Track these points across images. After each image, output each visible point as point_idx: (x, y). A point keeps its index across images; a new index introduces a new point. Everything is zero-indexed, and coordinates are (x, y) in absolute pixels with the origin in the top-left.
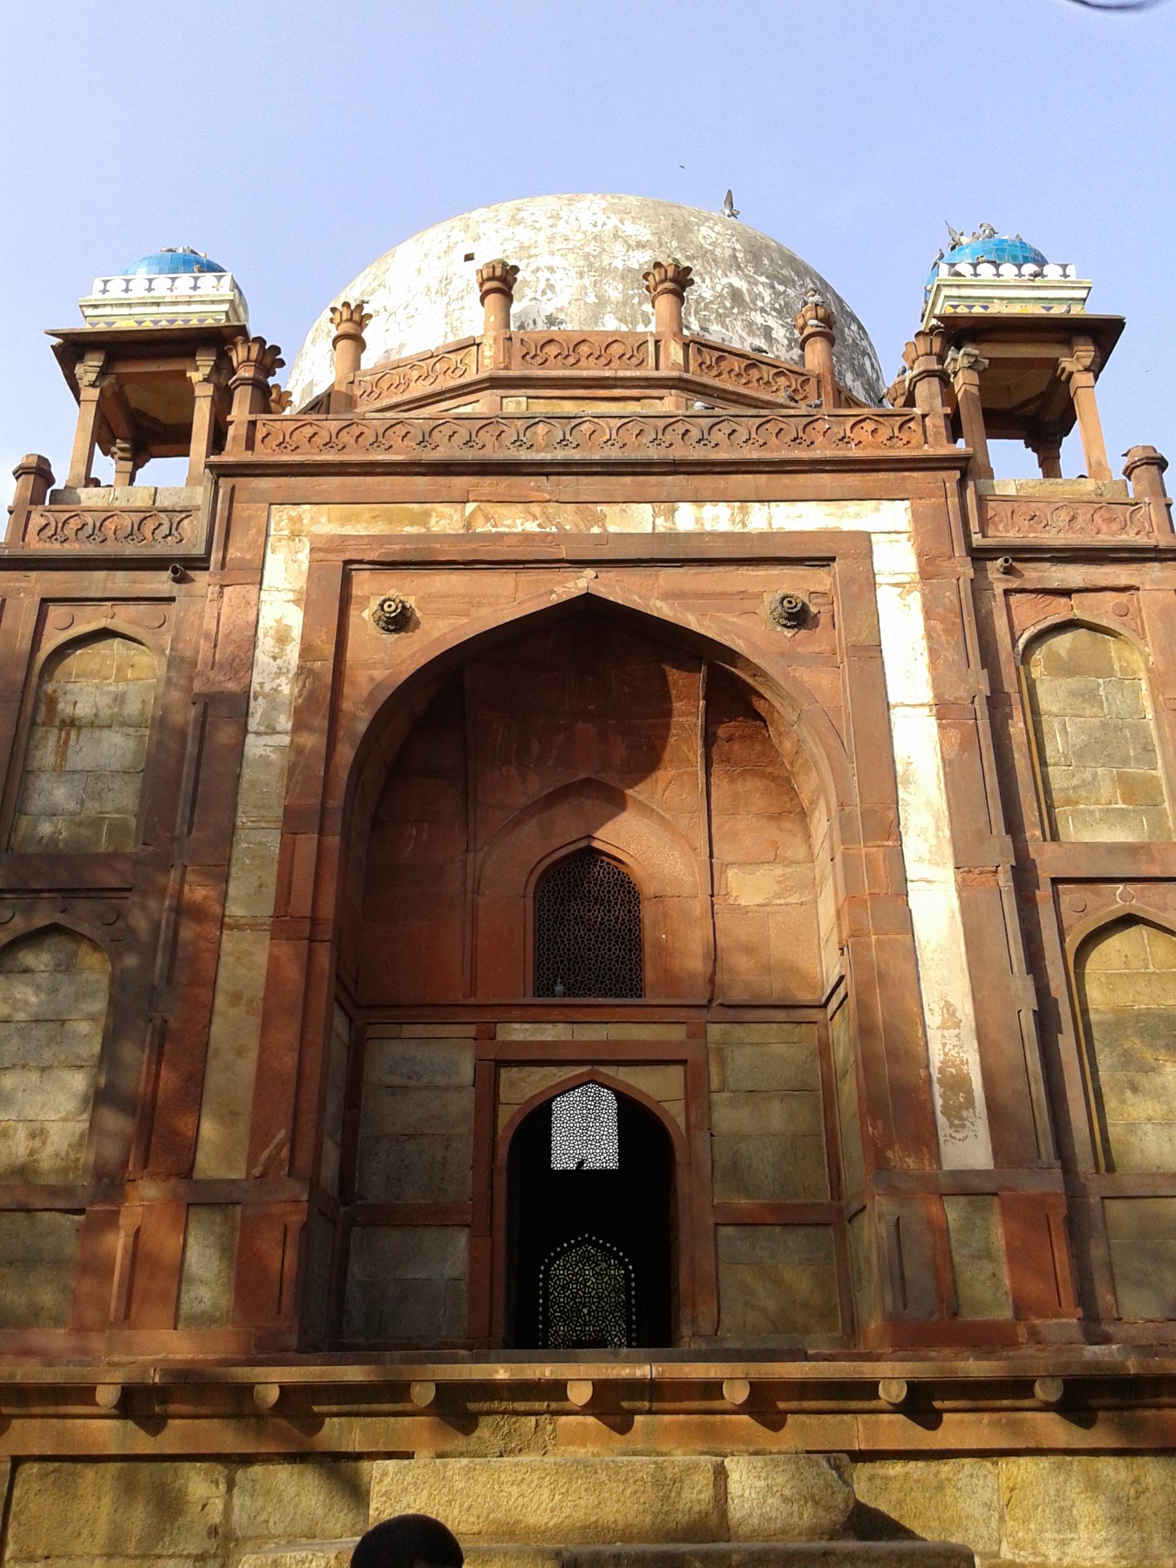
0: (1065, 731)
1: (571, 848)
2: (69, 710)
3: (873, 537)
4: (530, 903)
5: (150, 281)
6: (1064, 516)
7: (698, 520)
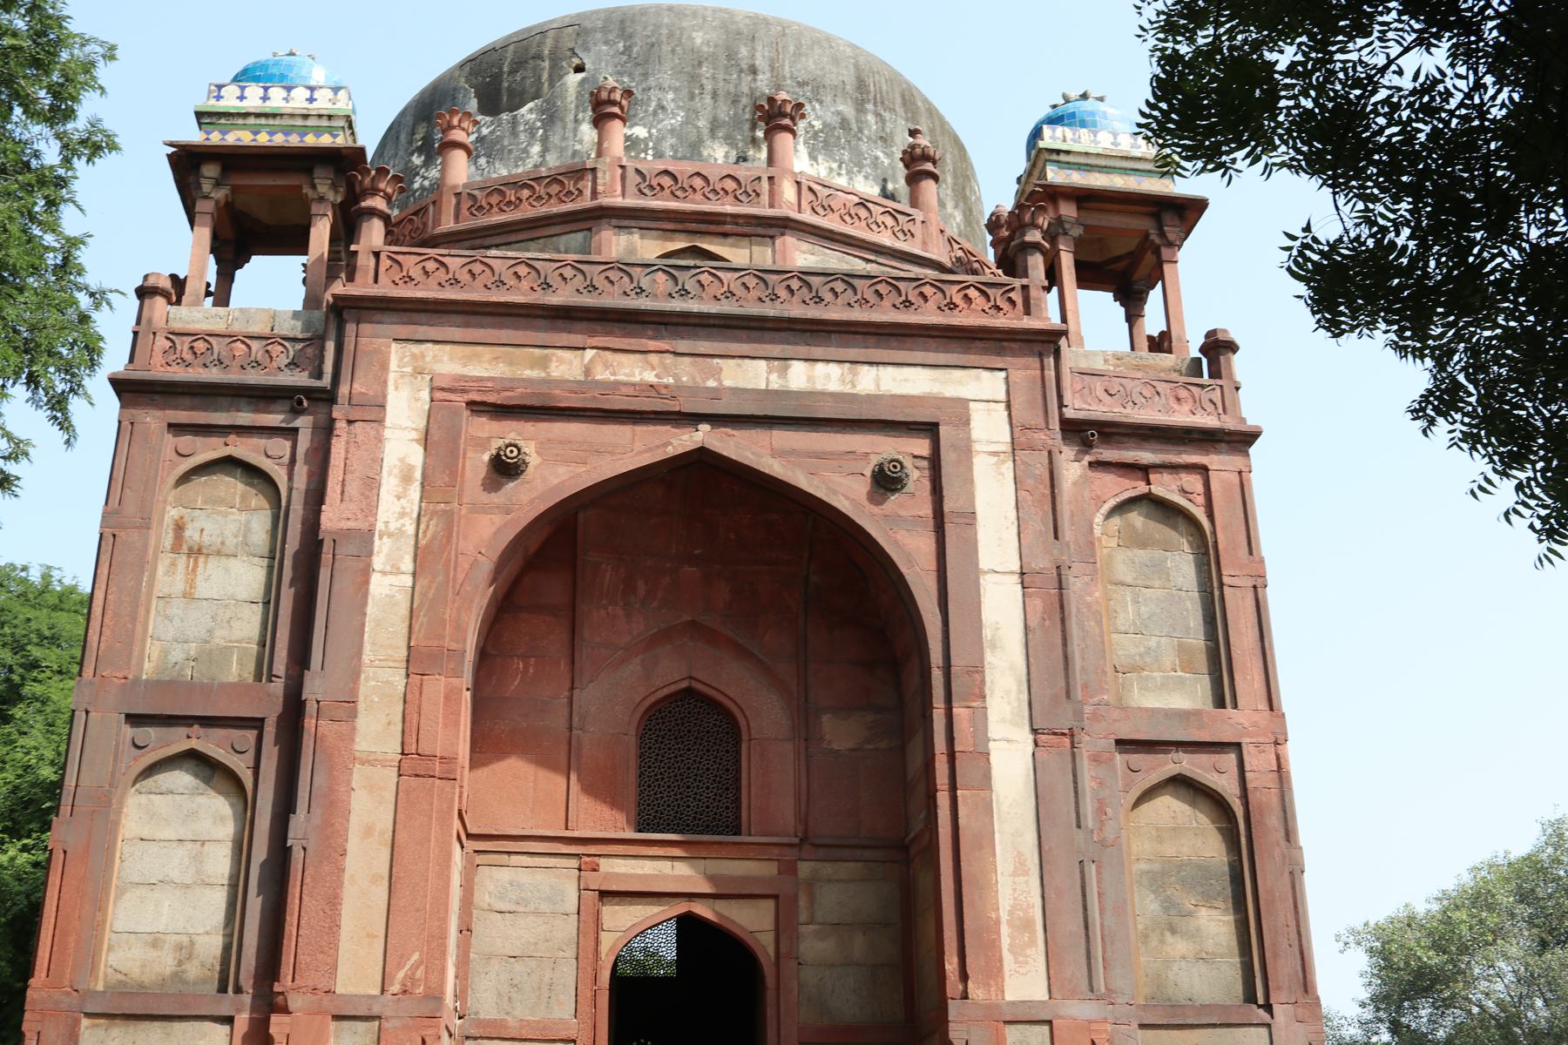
2: (196, 537)
3: (972, 405)
7: (810, 379)
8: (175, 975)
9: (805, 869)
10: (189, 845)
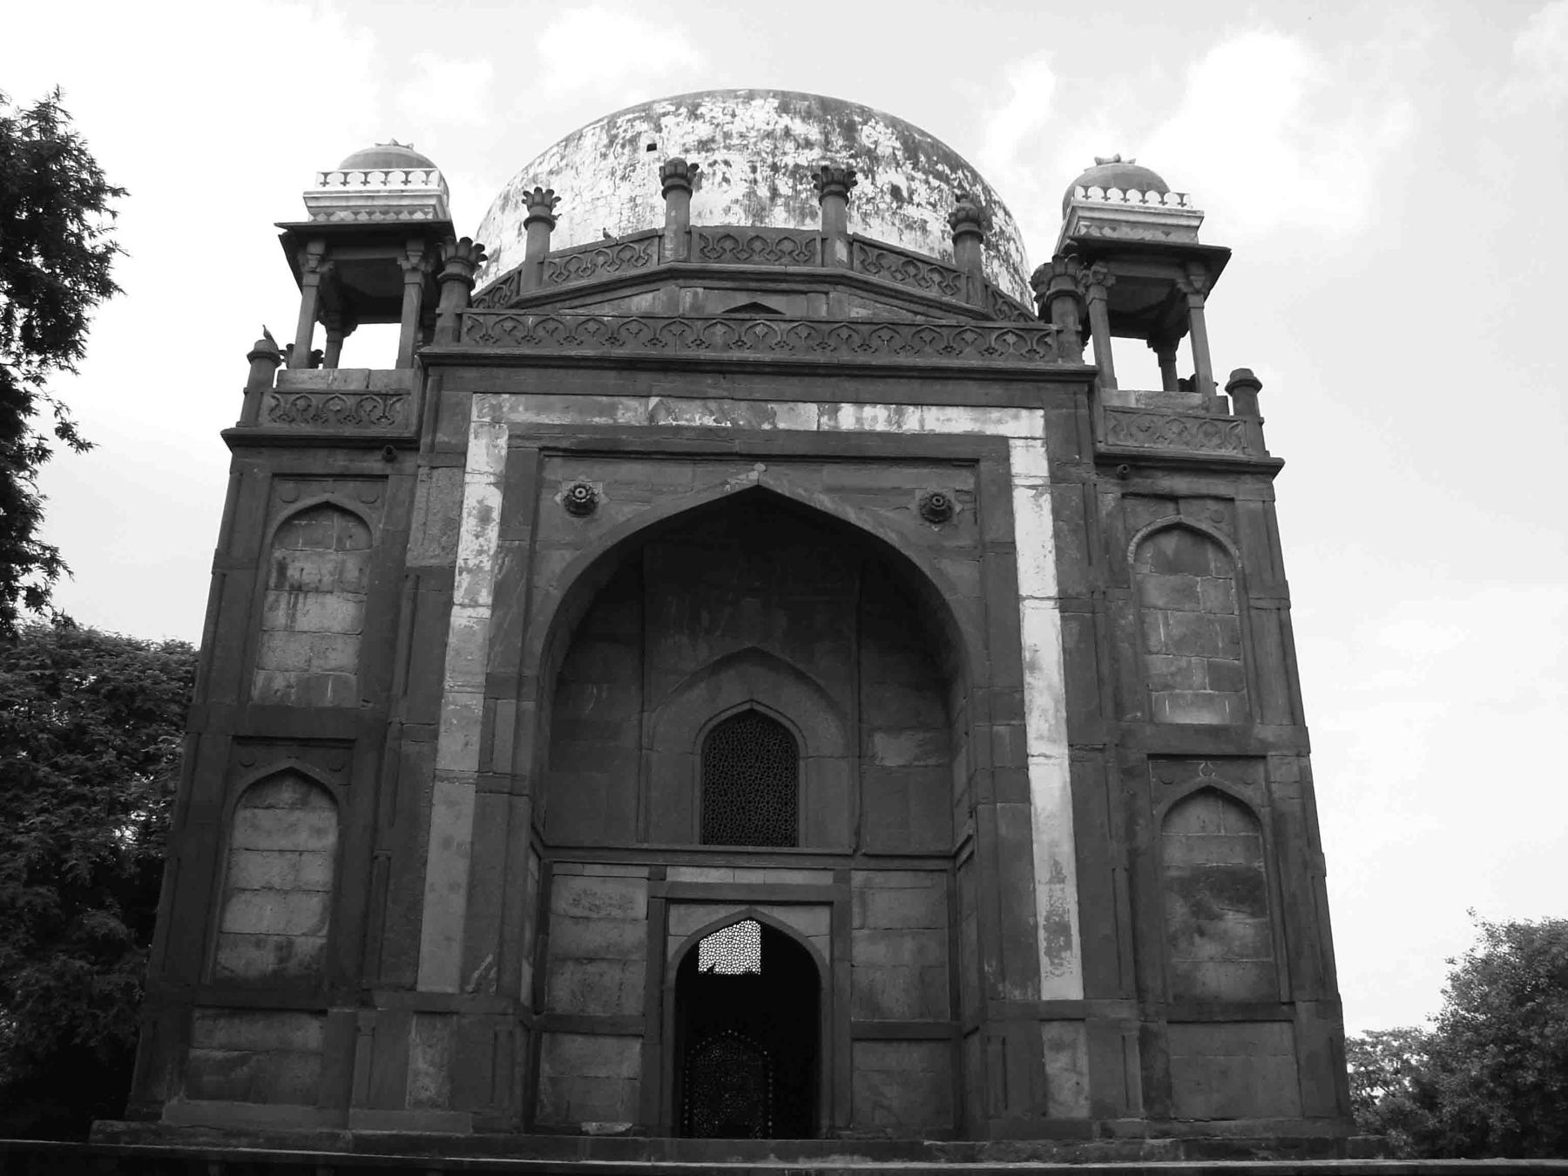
0: (1167, 624)
1: (735, 711)
2: (297, 576)
3: (1012, 442)
4: (698, 760)
5: (366, 174)
6: (1175, 428)
7: (859, 420)
8: (275, 972)
9: (858, 878)
10: (289, 855)
